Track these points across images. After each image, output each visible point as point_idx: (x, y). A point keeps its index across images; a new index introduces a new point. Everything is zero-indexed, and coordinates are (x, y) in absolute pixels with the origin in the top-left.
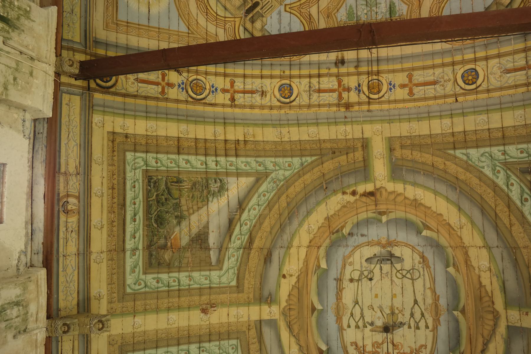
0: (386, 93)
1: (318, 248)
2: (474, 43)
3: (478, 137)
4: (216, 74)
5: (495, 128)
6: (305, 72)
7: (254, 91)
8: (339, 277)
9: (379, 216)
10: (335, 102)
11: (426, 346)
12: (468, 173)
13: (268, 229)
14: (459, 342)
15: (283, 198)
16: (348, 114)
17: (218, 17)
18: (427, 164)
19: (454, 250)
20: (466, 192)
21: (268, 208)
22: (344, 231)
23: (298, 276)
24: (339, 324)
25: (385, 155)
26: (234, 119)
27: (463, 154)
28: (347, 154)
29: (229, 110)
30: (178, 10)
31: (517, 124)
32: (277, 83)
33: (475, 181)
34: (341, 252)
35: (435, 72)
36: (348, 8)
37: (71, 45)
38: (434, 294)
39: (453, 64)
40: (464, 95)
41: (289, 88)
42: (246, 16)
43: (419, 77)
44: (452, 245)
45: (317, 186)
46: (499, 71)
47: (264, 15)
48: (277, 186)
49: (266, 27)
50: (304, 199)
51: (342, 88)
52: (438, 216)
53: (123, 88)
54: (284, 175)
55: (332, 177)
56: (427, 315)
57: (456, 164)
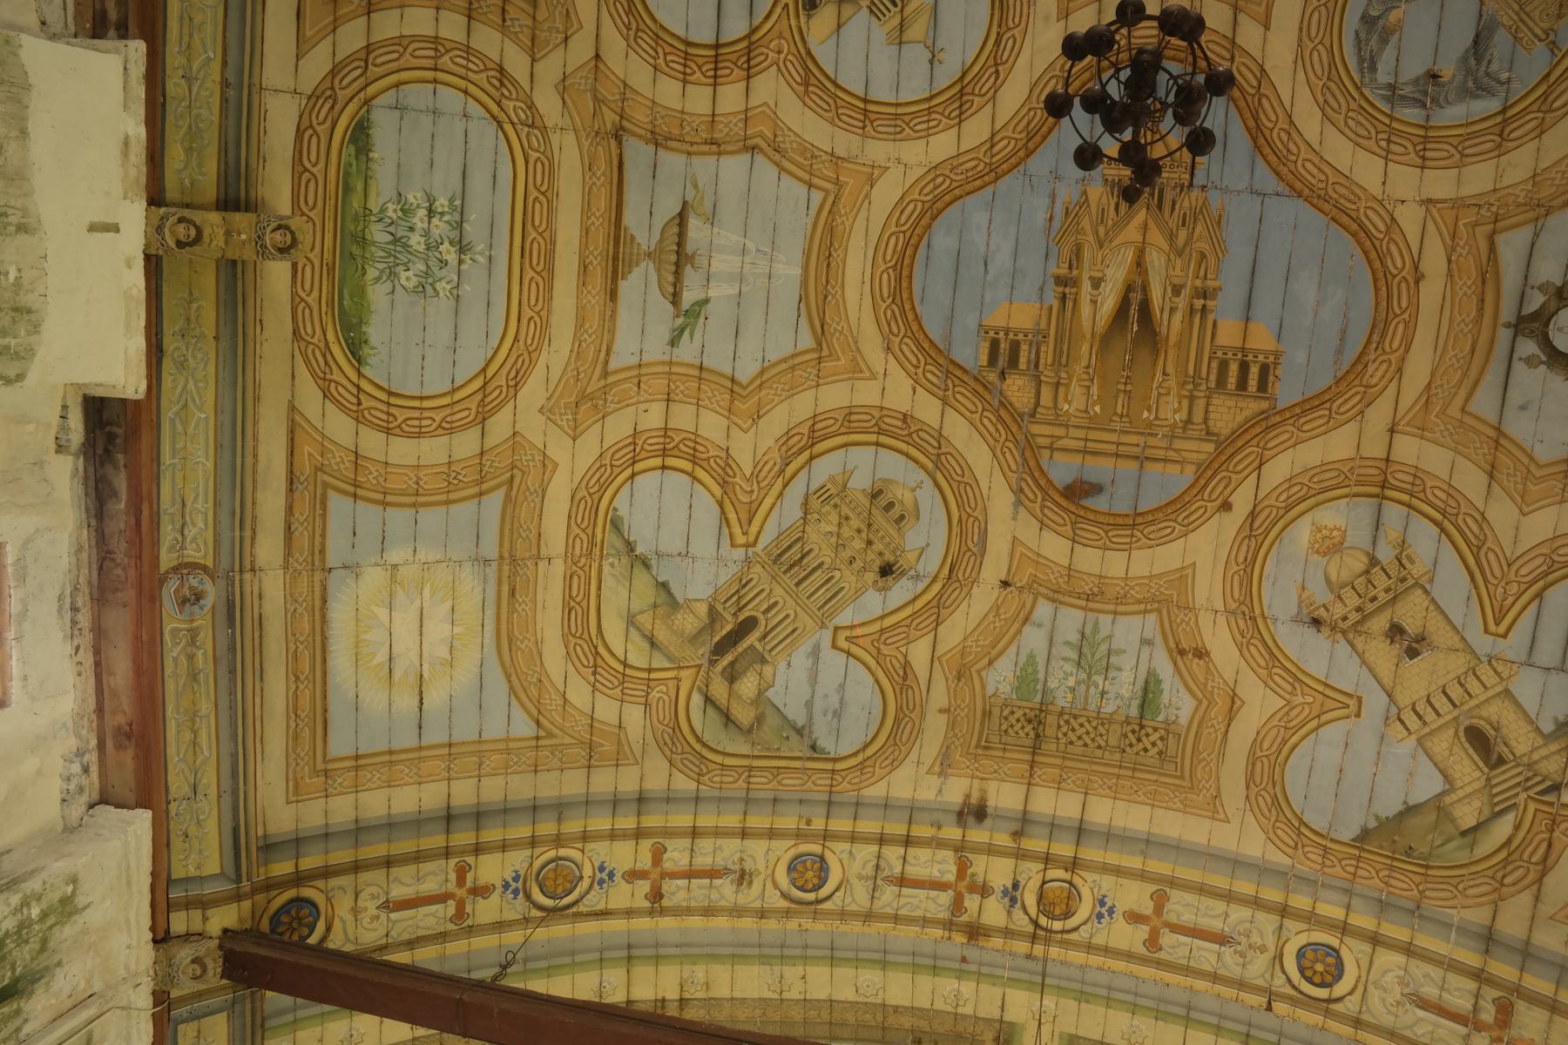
0: (1085, 923)
2: (1352, 882)
4: (613, 835)
6: (869, 826)
7: (719, 871)
10: (941, 916)
16: (972, 953)
17: (628, 671)
26: (657, 945)
29: (643, 923)
30: (508, 677)
32: (784, 850)
35: (1230, 912)
36: (1022, 659)
37: (194, 891)
39: (1284, 911)
40: (1293, 1002)
41: (818, 865)
42: (712, 663)
43: (1182, 907)
46: (1398, 989)
47: (766, 656)
49: (770, 694)
51: (965, 883)
53: (348, 940)
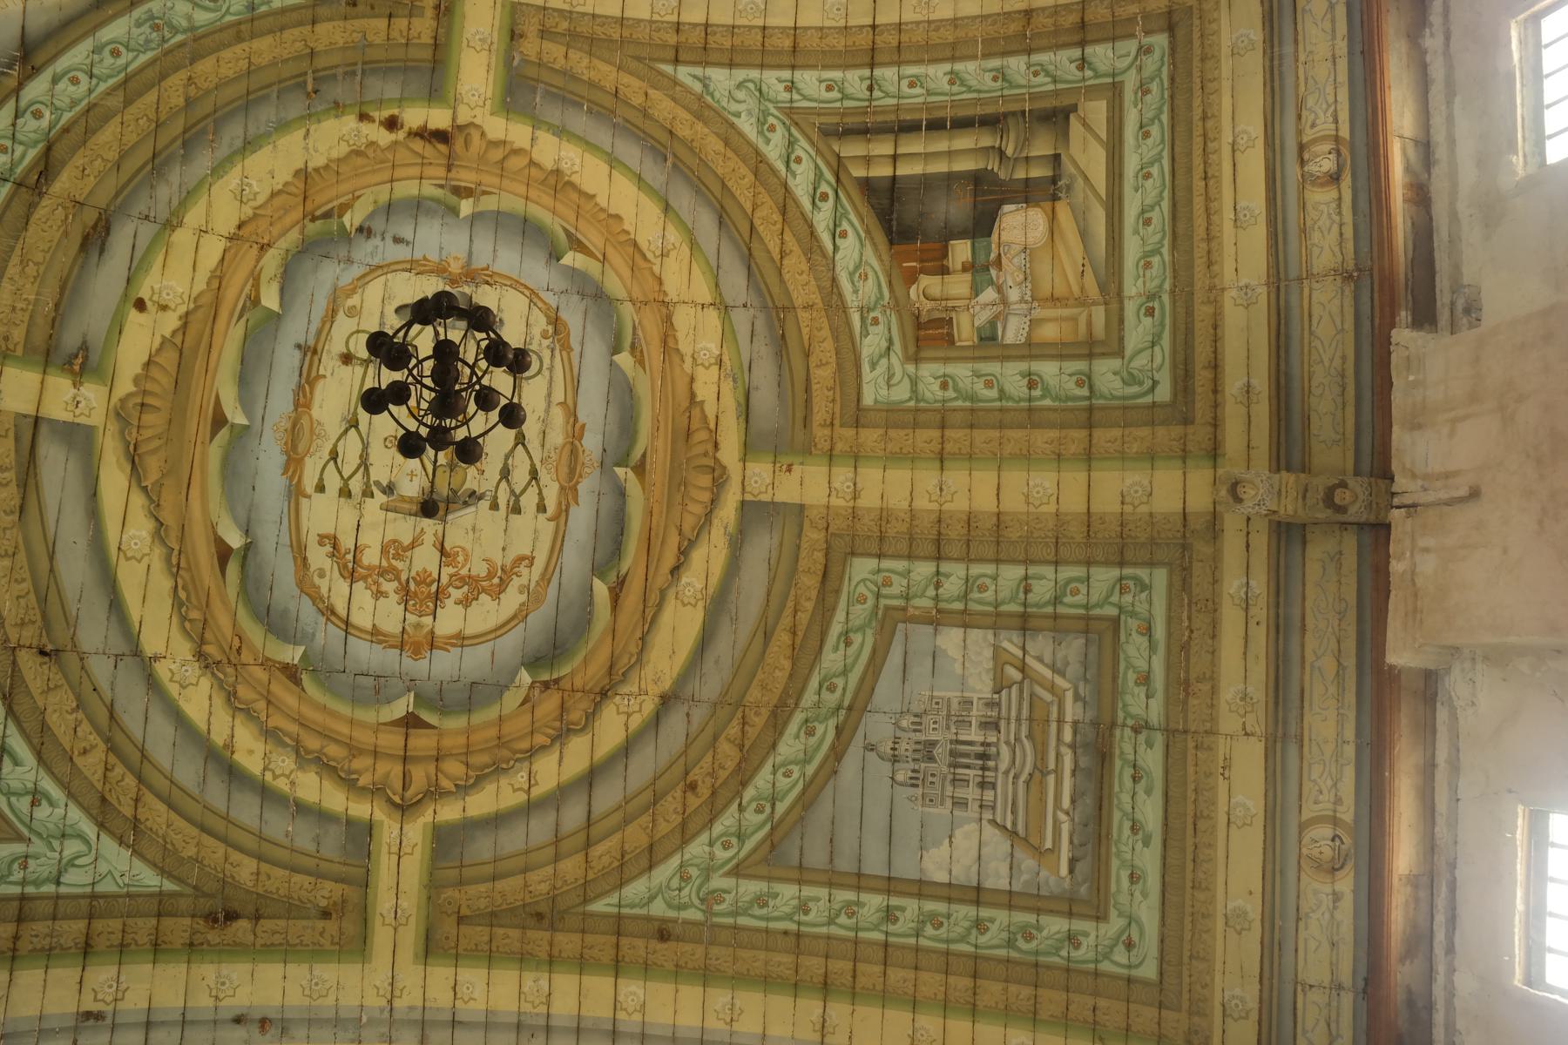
1: (262, 248)
3: (737, 41)
5: (778, 28)
8: (311, 342)
9: (453, 199)
11: (533, 558)
12: (701, 124)
13: (112, 155)
14: (619, 549)
15: (176, 81)
18: (602, 89)
19: (638, 311)
20: (688, 167)
21: (121, 93)
22: (346, 219)
23: (187, 314)
24: (291, 480)
25: (495, 47)
27: (695, 77)
28: (390, 16)
31: (828, 23)
33: (714, 145)
34: (327, 275)
38: (572, 420)
44: (634, 296)
45: (286, 80)
48: (164, 40)
50: (240, 102)
52: (611, 221)
54: (189, 18)
55: (336, 67)
56: (544, 476)
57: (674, 99)
